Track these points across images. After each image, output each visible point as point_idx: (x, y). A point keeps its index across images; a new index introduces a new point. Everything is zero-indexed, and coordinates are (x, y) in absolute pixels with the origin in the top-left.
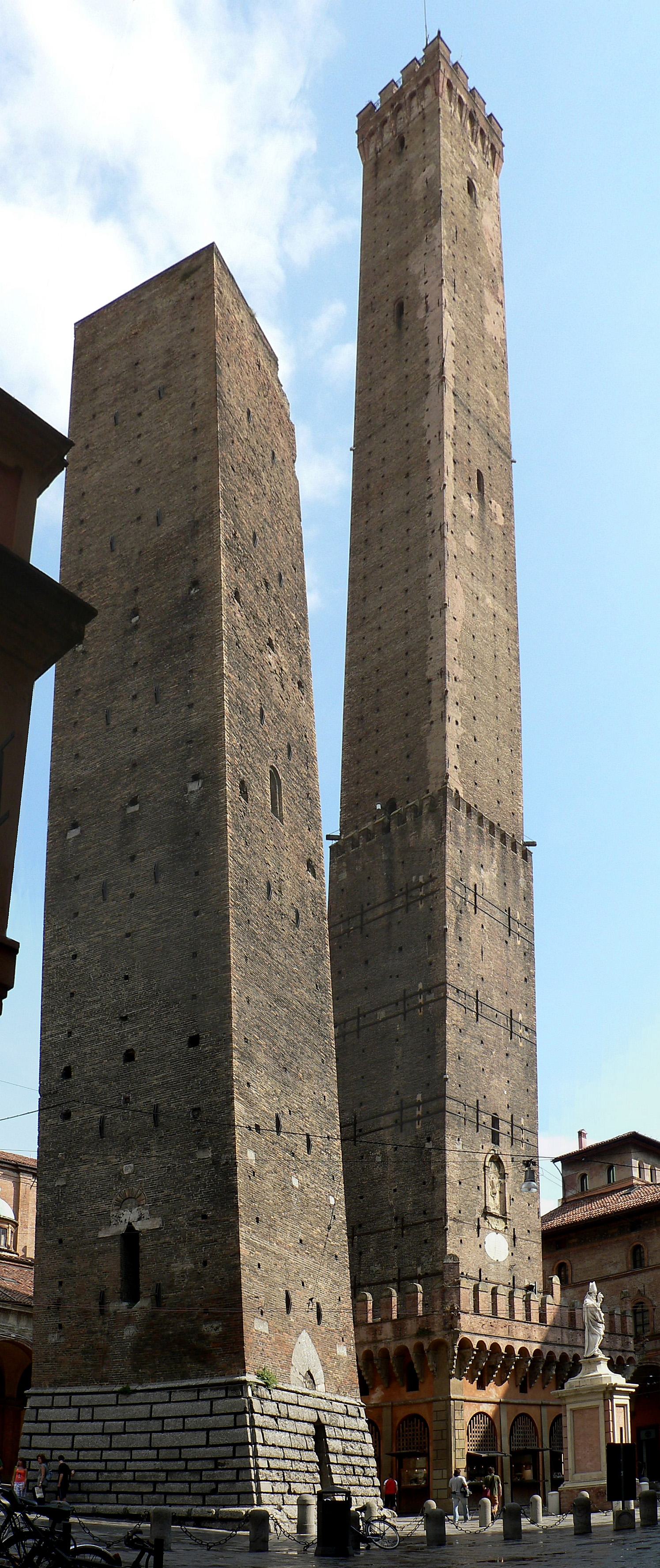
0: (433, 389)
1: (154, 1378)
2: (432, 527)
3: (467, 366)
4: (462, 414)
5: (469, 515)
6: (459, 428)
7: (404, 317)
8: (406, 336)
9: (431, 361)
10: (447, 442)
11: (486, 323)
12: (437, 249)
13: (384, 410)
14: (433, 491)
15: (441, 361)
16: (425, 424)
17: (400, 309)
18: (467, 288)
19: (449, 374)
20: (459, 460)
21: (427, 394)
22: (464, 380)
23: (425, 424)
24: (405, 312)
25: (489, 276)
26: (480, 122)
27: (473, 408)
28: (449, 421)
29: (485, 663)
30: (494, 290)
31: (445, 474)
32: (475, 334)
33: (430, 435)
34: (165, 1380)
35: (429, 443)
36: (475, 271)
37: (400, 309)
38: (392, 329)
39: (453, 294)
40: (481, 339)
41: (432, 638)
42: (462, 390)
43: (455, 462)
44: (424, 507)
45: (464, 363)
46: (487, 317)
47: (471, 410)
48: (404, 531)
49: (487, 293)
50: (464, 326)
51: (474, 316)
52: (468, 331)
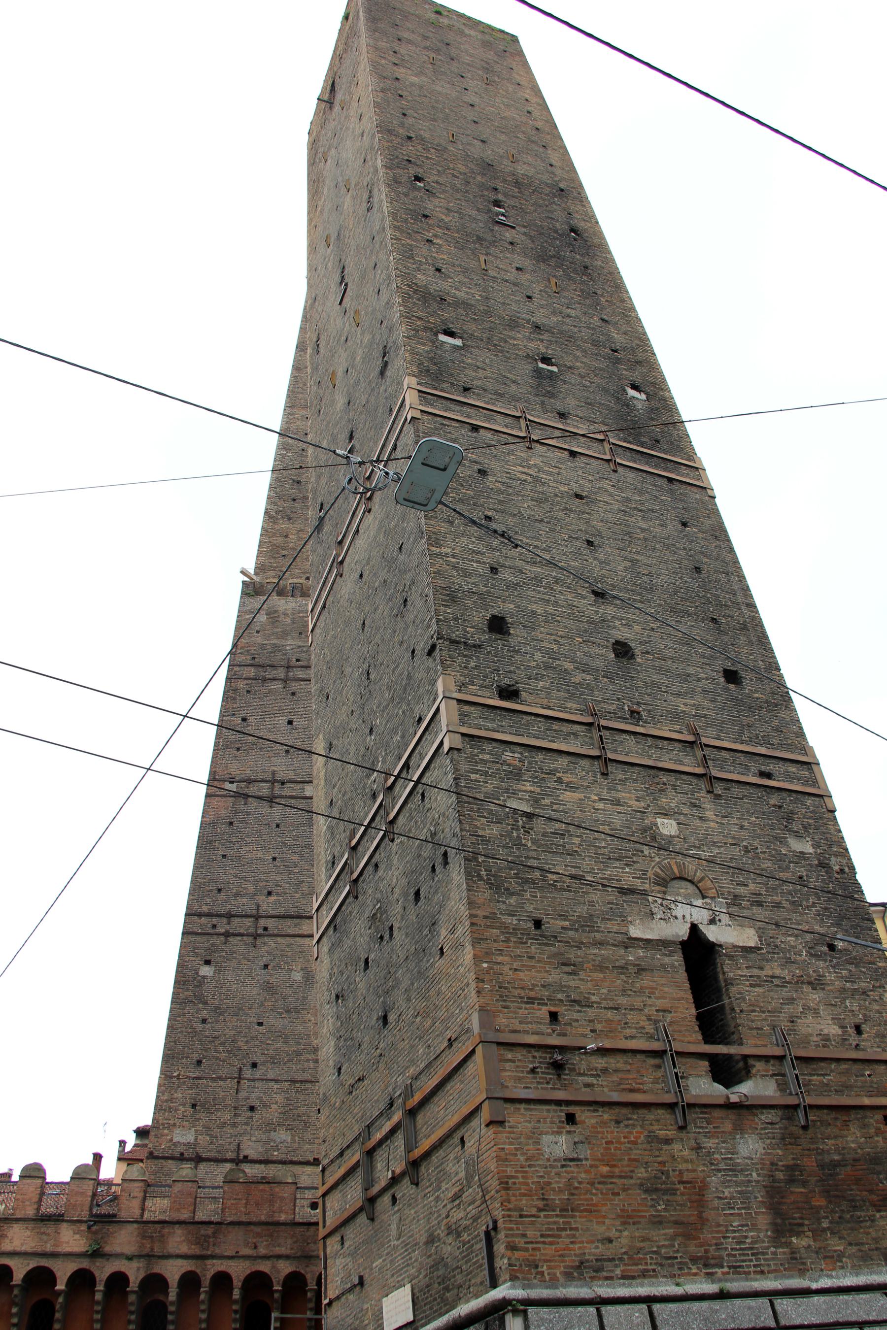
1: (835, 1260)
34: (856, 1270)
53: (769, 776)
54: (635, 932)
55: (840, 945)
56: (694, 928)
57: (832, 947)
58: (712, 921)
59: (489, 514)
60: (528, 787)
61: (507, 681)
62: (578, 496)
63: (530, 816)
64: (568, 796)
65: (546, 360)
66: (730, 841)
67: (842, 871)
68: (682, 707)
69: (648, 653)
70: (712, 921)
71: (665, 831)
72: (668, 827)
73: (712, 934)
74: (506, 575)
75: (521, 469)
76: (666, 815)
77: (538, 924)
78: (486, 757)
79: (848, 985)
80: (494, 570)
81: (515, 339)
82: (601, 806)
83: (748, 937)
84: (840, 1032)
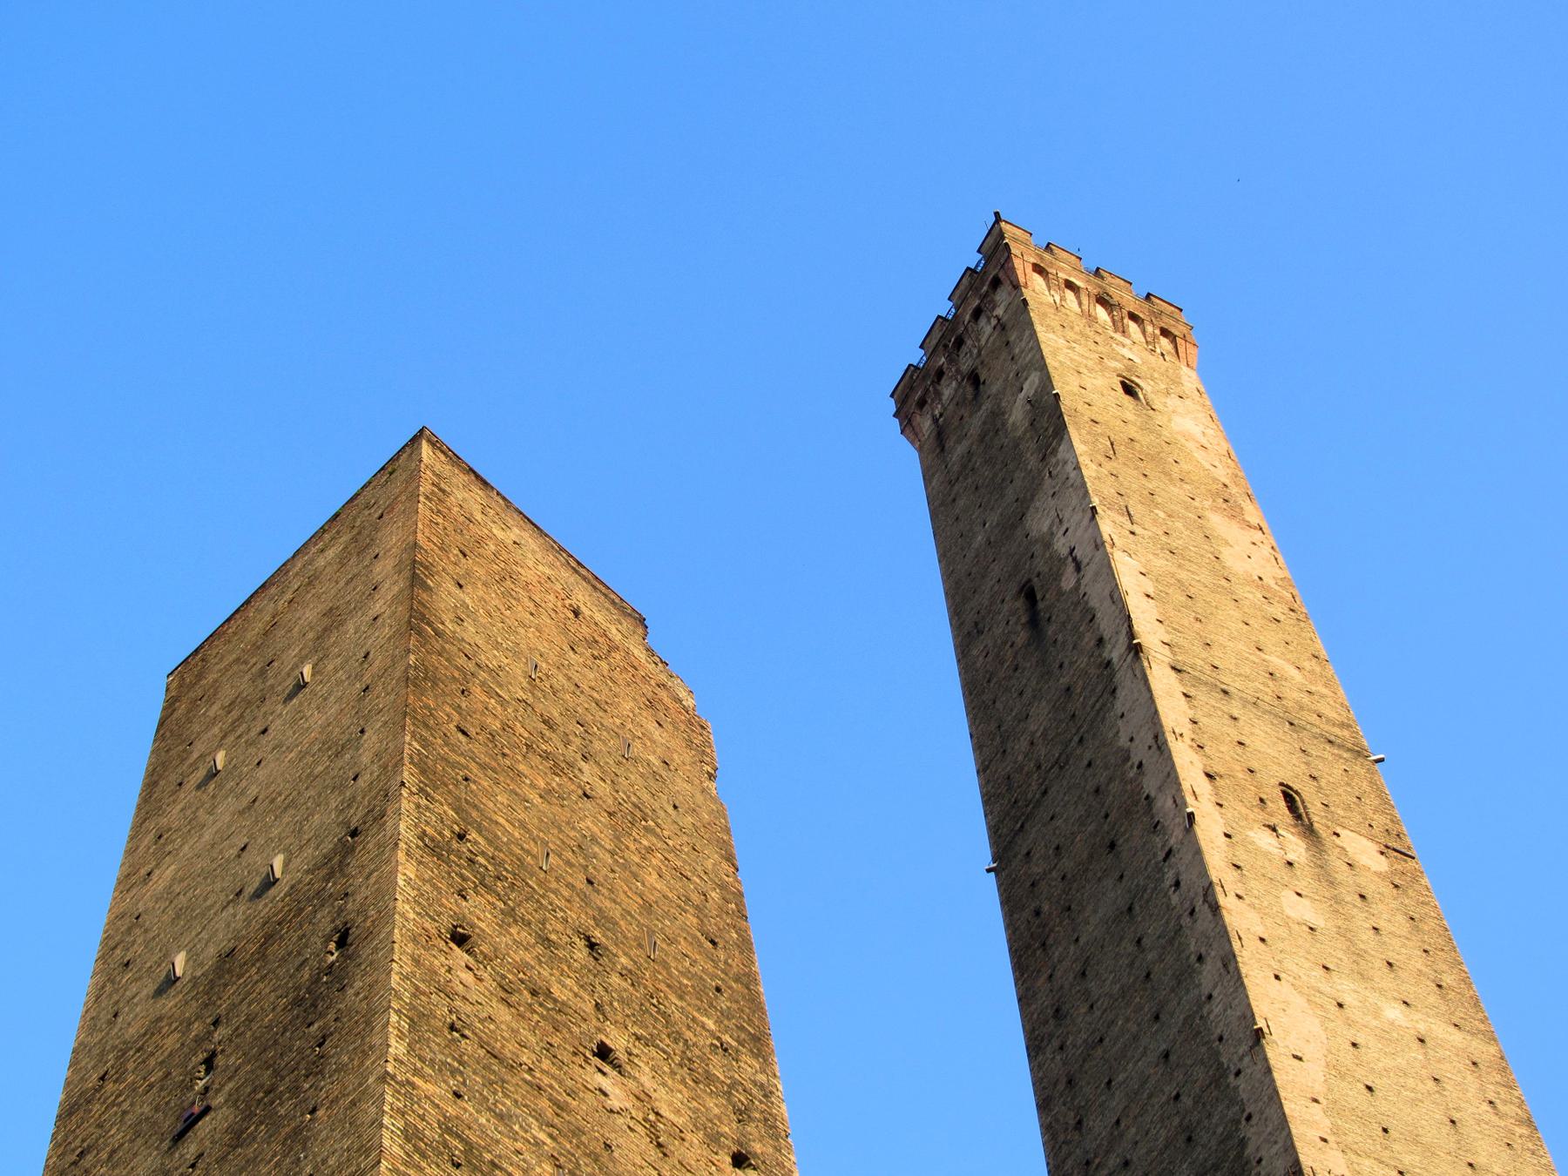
0: (1123, 677)
2: (1187, 905)
3: (1198, 625)
5: (1281, 864)
6: (1203, 721)
7: (1041, 605)
8: (1050, 630)
9: (1106, 637)
12: (1073, 475)
13: (1039, 767)
14: (1172, 841)
16: (1123, 741)
18: (1162, 515)
19: (1148, 631)
20: (1222, 771)
21: (1114, 691)
22: (1198, 648)
23: (1123, 741)
24: (1039, 597)
26: (1123, 303)
27: (1227, 680)
29: (1424, 1140)
31: (1189, 799)
32: (1205, 576)
33: (1139, 753)
35: (1140, 765)
37: (1029, 594)
38: (1022, 637)
39: (1129, 526)
40: (1224, 582)
41: (1249, 1118)
42: (1196, 658)
43: (1209, 776)
44: (1161, 880)
45: (1187, 620)
46: (1227, 555)
47: (1230, 689)
48: (1131, 948)
50: (1174, 569)
52: (1183, 575)
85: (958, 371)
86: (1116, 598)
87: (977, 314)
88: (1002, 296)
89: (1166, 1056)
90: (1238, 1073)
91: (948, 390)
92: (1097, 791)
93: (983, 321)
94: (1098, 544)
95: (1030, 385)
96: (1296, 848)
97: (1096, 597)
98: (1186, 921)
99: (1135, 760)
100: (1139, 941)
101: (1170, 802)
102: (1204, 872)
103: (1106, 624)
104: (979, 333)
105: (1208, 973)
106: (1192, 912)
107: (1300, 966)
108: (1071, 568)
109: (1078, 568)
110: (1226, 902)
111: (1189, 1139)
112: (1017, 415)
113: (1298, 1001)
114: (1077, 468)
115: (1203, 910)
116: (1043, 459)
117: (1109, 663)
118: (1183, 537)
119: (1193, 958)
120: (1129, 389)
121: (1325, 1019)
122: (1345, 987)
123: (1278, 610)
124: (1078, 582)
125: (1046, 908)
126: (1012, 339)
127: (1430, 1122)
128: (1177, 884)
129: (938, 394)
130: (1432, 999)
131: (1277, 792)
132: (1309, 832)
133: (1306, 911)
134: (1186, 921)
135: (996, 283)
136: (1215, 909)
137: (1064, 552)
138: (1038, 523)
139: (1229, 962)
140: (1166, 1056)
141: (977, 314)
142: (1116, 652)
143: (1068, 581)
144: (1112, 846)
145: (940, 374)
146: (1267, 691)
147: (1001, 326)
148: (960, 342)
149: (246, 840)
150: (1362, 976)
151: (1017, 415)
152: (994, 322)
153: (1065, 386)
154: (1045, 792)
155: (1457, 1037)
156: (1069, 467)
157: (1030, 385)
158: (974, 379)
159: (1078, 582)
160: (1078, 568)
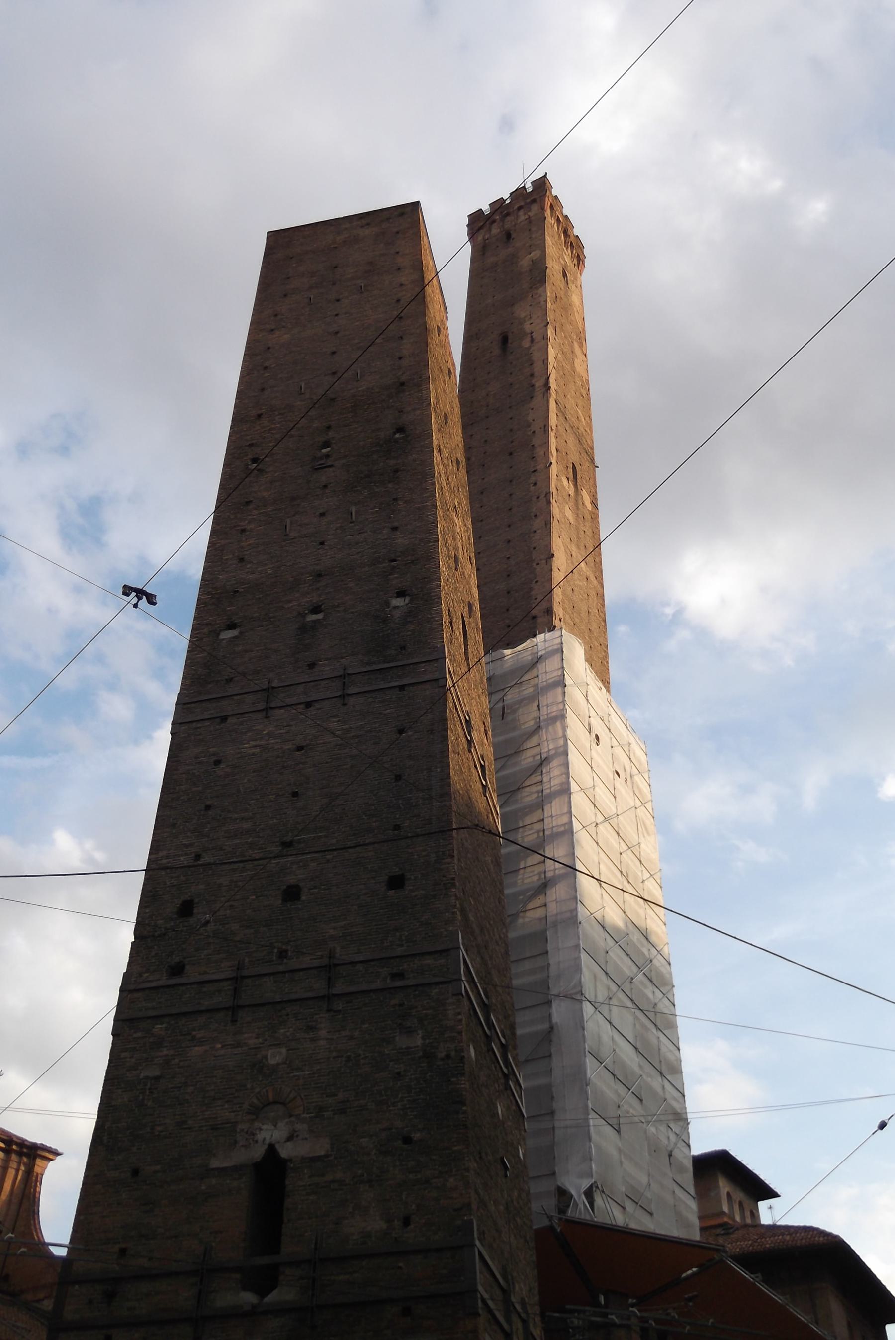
4: (561, 418)
9: (536, 374)
10: (552, 435)
11: (576, 365)
15: (545, 377)
16: (530, 418)
17: (505, 340)
19: (553, 384)
21: (532, 397)
23: (530, 418)
24: (510, 341)
25: (577, 335)
28: (553, 420)
30: (581, 346)
35: (534, 432)
36: (569, 327)
38: (497, 351)
46: (576, 361)
49: (576, 345)
51: (568, 356)
53: (400, 975)
54: (215, 1163)
55: (417, 1136)
56: (272, 1149)
57: (407, 1140)
58: (290, 1138)
59: (208, 803)
60: (165, 1051)
61: (177, 959)
62: (300, 748)
63: (157, 1078)
64: (198, 1050)
65: (316, 610)
66: (334, 1054)
67: (448, 1056)
68: (332, 932)
69: (315, 887)
70: (290, 1138)
71: (272, 1061)
72: (275, 1057)
73: (285, 1151)
74: (206, 858)
75: (253, 743)
76: (279, 1045)
77: (136, 1172)
78: (139, 1034)
79: (411, 1176)
80: (198, 857)
81: (290, 601)
82: (222, 1052)
83: (321, 1147)
84: (384, 1225)
85: (503, 226)
86: (545, 361)
87: (520, 208)
88: (535, 208)
89: (509, 542)
90: (538, 564)
91: (495, 230)
92: (511, 430)
93: (521, 213)
94: (545, 338)
95: (535, 254)
96: (572, 492)
97: (536, 356)
98: (534, 499)
99: (533, 428)
100: (511, 495)
101: (542, 453)
102: (549, 486)
103: (537, 368)
104: (518, 217)
105: (537, 523)
106: (538, 498)
107: (564, 535)
108: (528, 339)
109: (532, 340)
110: (553, 501)
111: (509, 576)
112: (525, 262)
113: (563, 548)
114: (546, 301)
115: (543, 500)
116: (531, 288)
117: (533, 386)
118: (567, 349)
119: (533, 514)
120: (565, 275)
121: (567, 559)
122: (574, 549)
123: (584, 392)
124: (530, 347)
125: (473, 459)
126: (534, 229)
127: (584, 608)
128: (535, 484)
129: (490, 230)
130: (592, 565)
131: (571, 465)
132: (576, 485)
133: (569, 514)
134: (534, 499)
135: (534, 201)
136: (549, 502)
137: (528, 331)
138: (521, 311)
139: (548, 524)
140: (509, 542)
141: (520, 208)
142: (539, 384)
143: (526, 343)
144: (511, 454)
145: (494, 222)
146: (576, 423)
147: (530, 220)
148: (508, 214)
149: (334, 349)
150: (578, 547)
151: (525, 262)
152: (527, 217)
153: (550, 263)
154: (487, 417)
155: (595, 582)
156: (542, 299)
157: (535, 254)
158: (508, 236)
159: (530, 347)
160: (532, 340)
